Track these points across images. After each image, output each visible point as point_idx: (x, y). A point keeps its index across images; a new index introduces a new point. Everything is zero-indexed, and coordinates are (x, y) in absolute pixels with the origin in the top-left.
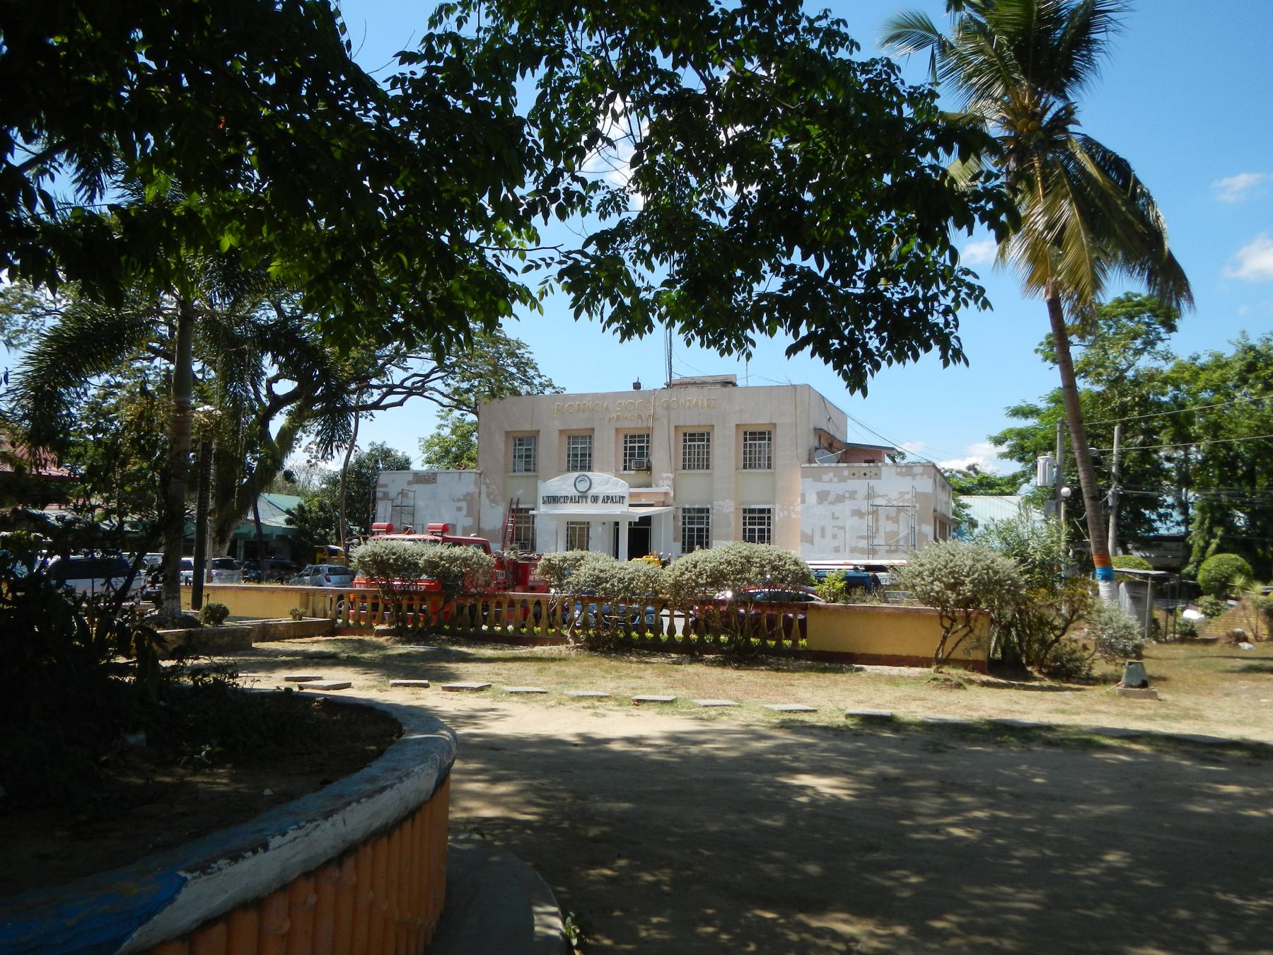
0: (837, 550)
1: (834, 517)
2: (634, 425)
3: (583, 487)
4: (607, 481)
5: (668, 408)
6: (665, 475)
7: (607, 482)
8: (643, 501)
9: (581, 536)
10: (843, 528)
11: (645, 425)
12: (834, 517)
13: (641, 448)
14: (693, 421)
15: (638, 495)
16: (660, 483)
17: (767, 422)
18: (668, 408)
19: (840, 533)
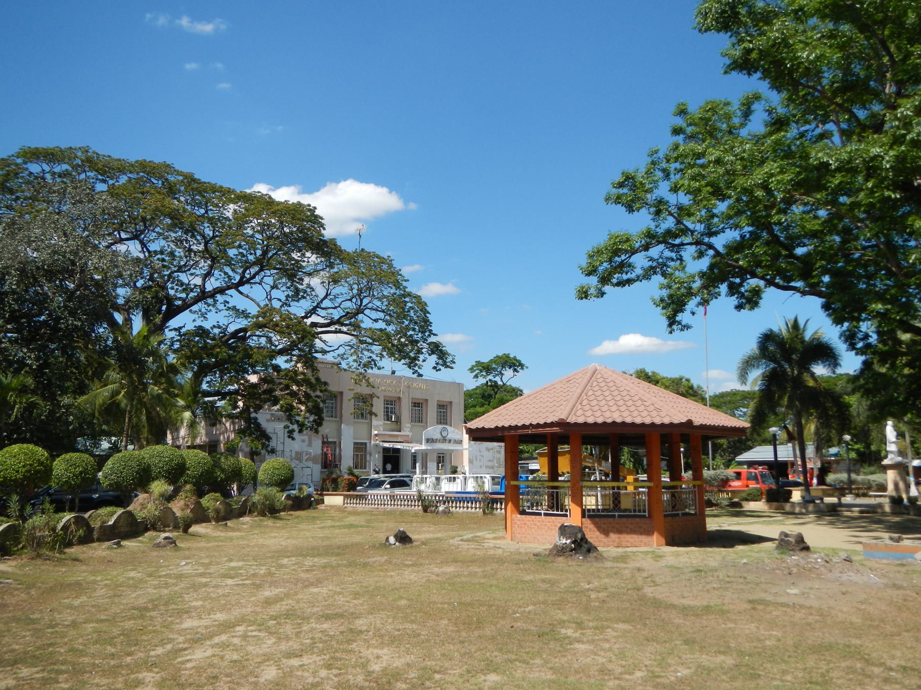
0: (481, 467)
1: (480, 451)
2: (393, 394)
3: (444, 434)
4: (379, 426)
5: (409, 387)
6: (407, 425)
7: (454, 432)
8: (400, 440)
9: (361, 459)
10: (482, 456)
11: (398, 396)
12: (480, 451)
13: (392, 408)
14: (419, 396)
15: (397, 436)
16: (405, 429)
17: (448, 400)
18: (409, 387)
19: (482, 458)
